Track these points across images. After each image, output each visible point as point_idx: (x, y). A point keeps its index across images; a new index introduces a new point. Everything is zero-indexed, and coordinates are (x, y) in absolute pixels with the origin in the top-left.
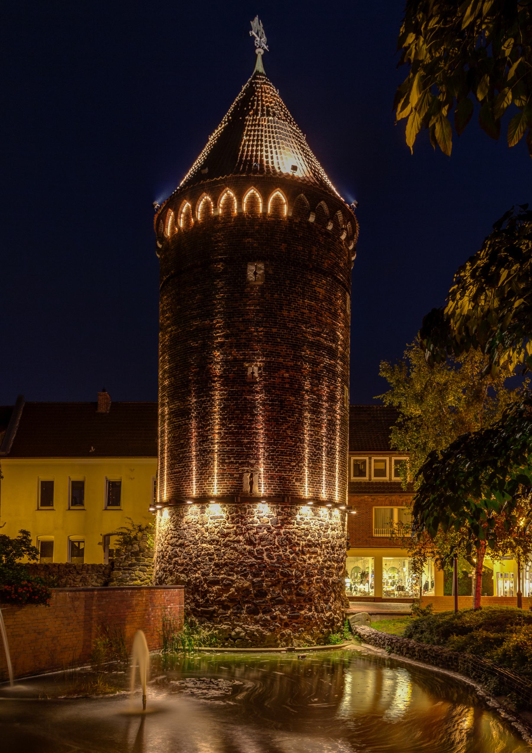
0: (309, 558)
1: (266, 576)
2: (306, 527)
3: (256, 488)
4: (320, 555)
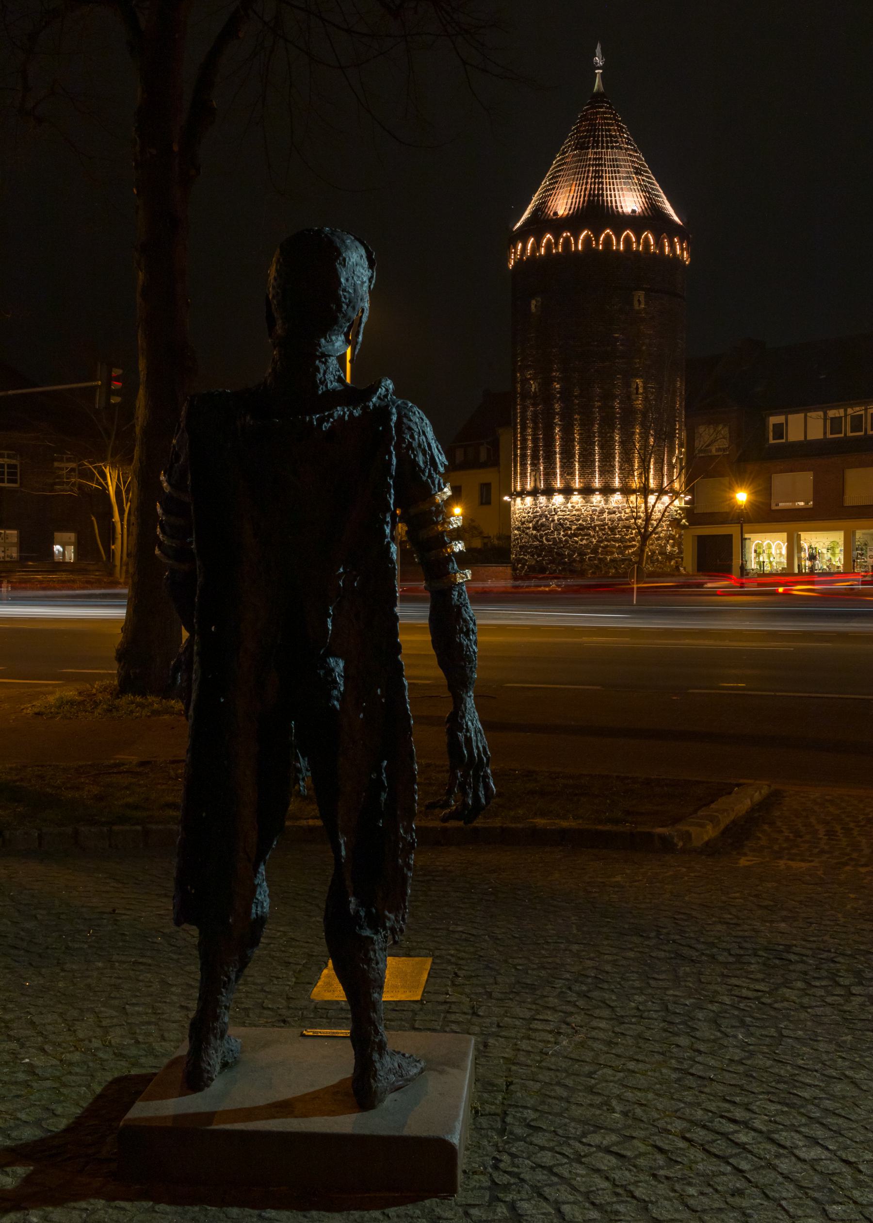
0: (582, 540)
1: (545, 556)
2: (577, 513)
3: (538, 484)
4: (594, 536)
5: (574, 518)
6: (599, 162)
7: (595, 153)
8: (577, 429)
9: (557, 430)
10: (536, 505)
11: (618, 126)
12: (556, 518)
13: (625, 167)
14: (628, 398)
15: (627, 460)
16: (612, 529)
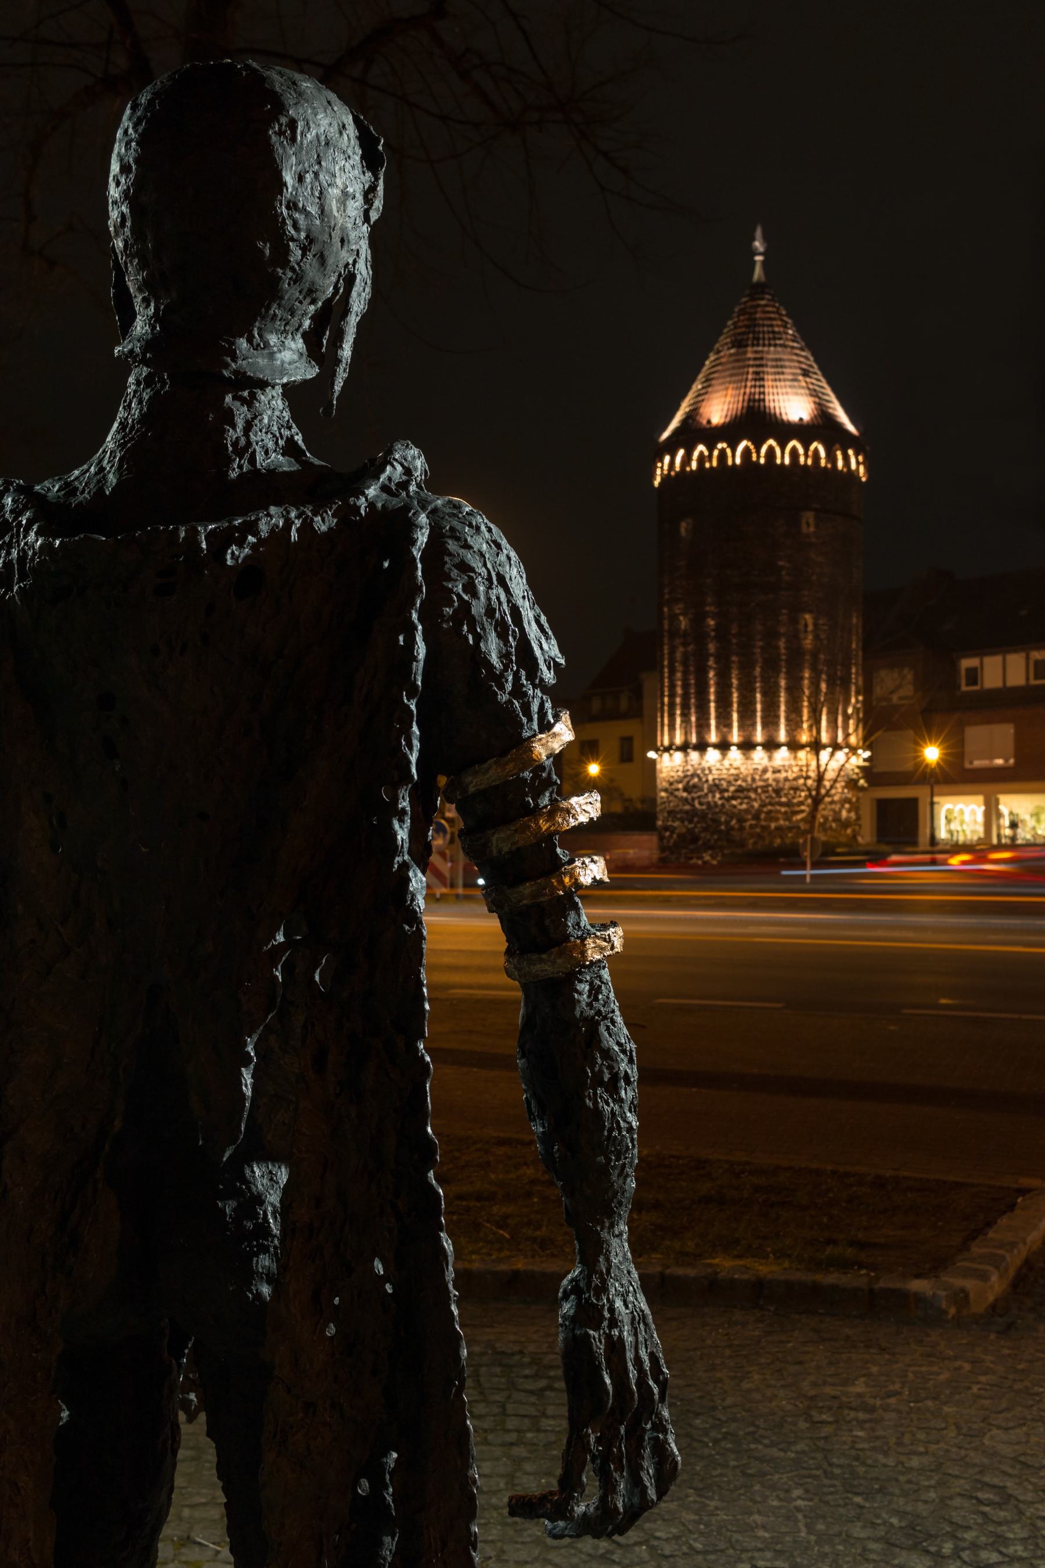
0: (741, 804)
1: (698, 822)
4: (755, 800)
5: (732, 778)
6: (760, 362)
7: (756, 352)
8: (734, 673)
9: (711, 674)
10: (686, 762)
11: (782, 320)
12: (710, 778)
13: (791, 367)
14: (795, 638)
15: (794, 709)
16: (778, 791)
